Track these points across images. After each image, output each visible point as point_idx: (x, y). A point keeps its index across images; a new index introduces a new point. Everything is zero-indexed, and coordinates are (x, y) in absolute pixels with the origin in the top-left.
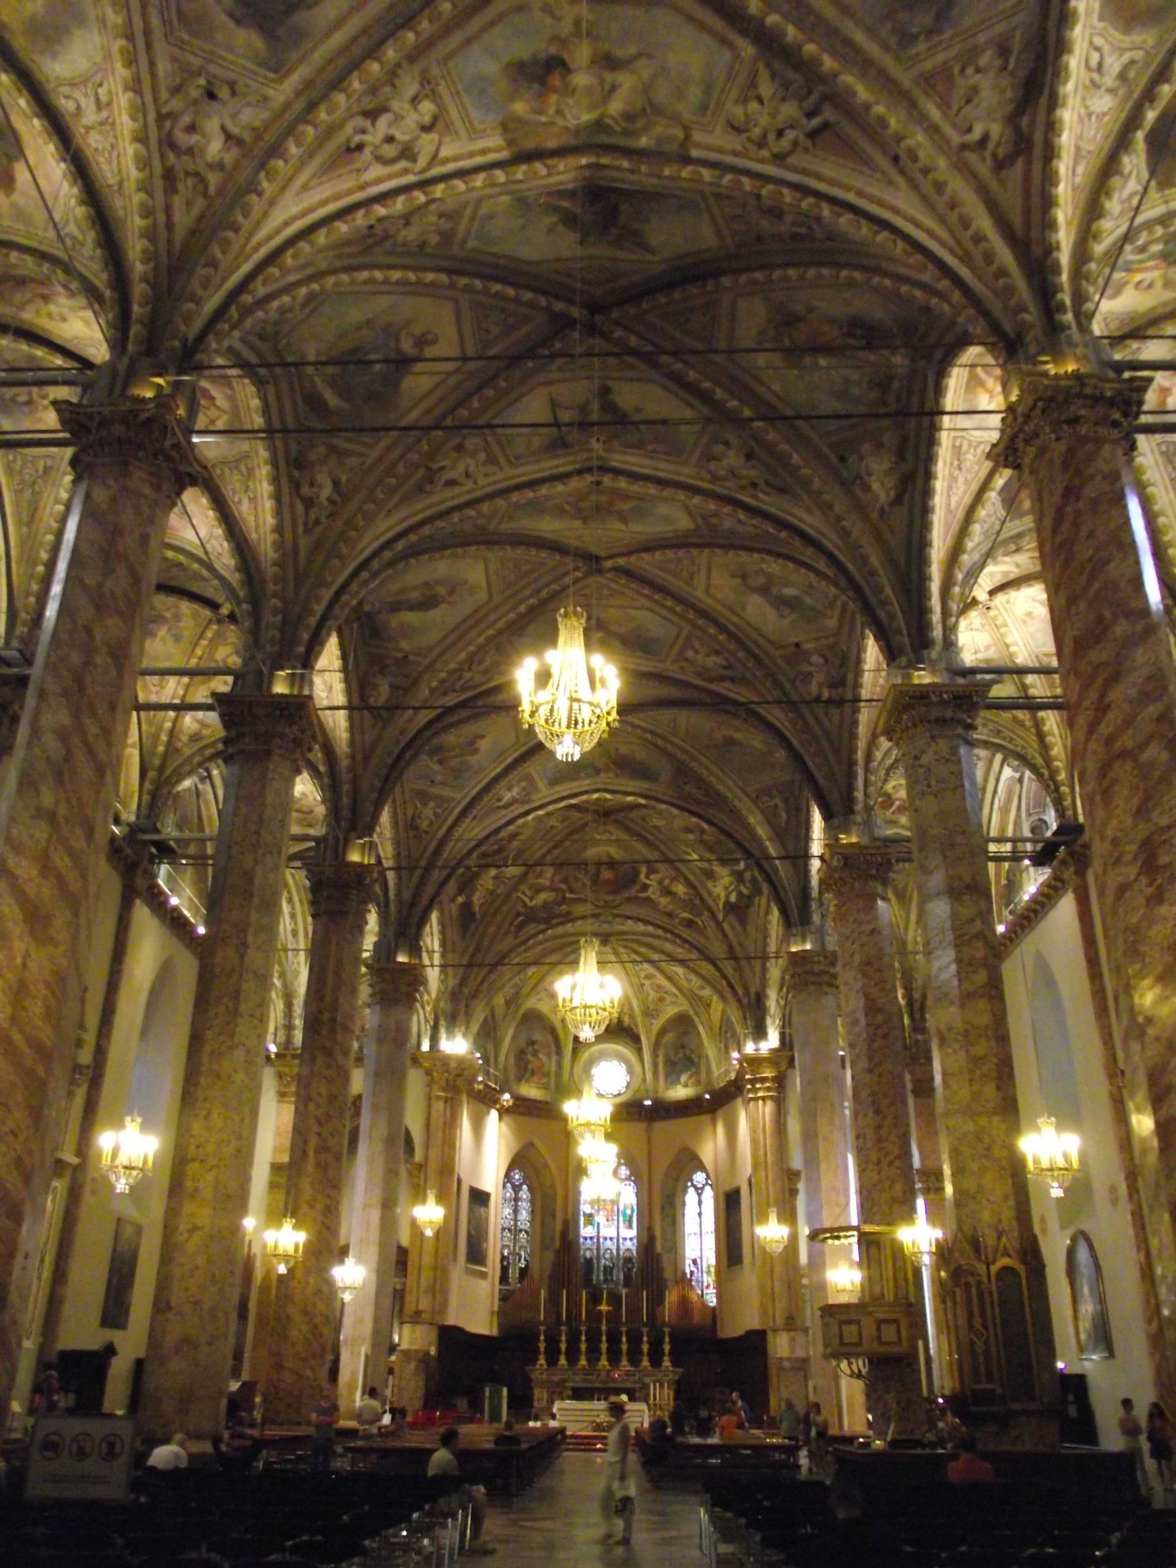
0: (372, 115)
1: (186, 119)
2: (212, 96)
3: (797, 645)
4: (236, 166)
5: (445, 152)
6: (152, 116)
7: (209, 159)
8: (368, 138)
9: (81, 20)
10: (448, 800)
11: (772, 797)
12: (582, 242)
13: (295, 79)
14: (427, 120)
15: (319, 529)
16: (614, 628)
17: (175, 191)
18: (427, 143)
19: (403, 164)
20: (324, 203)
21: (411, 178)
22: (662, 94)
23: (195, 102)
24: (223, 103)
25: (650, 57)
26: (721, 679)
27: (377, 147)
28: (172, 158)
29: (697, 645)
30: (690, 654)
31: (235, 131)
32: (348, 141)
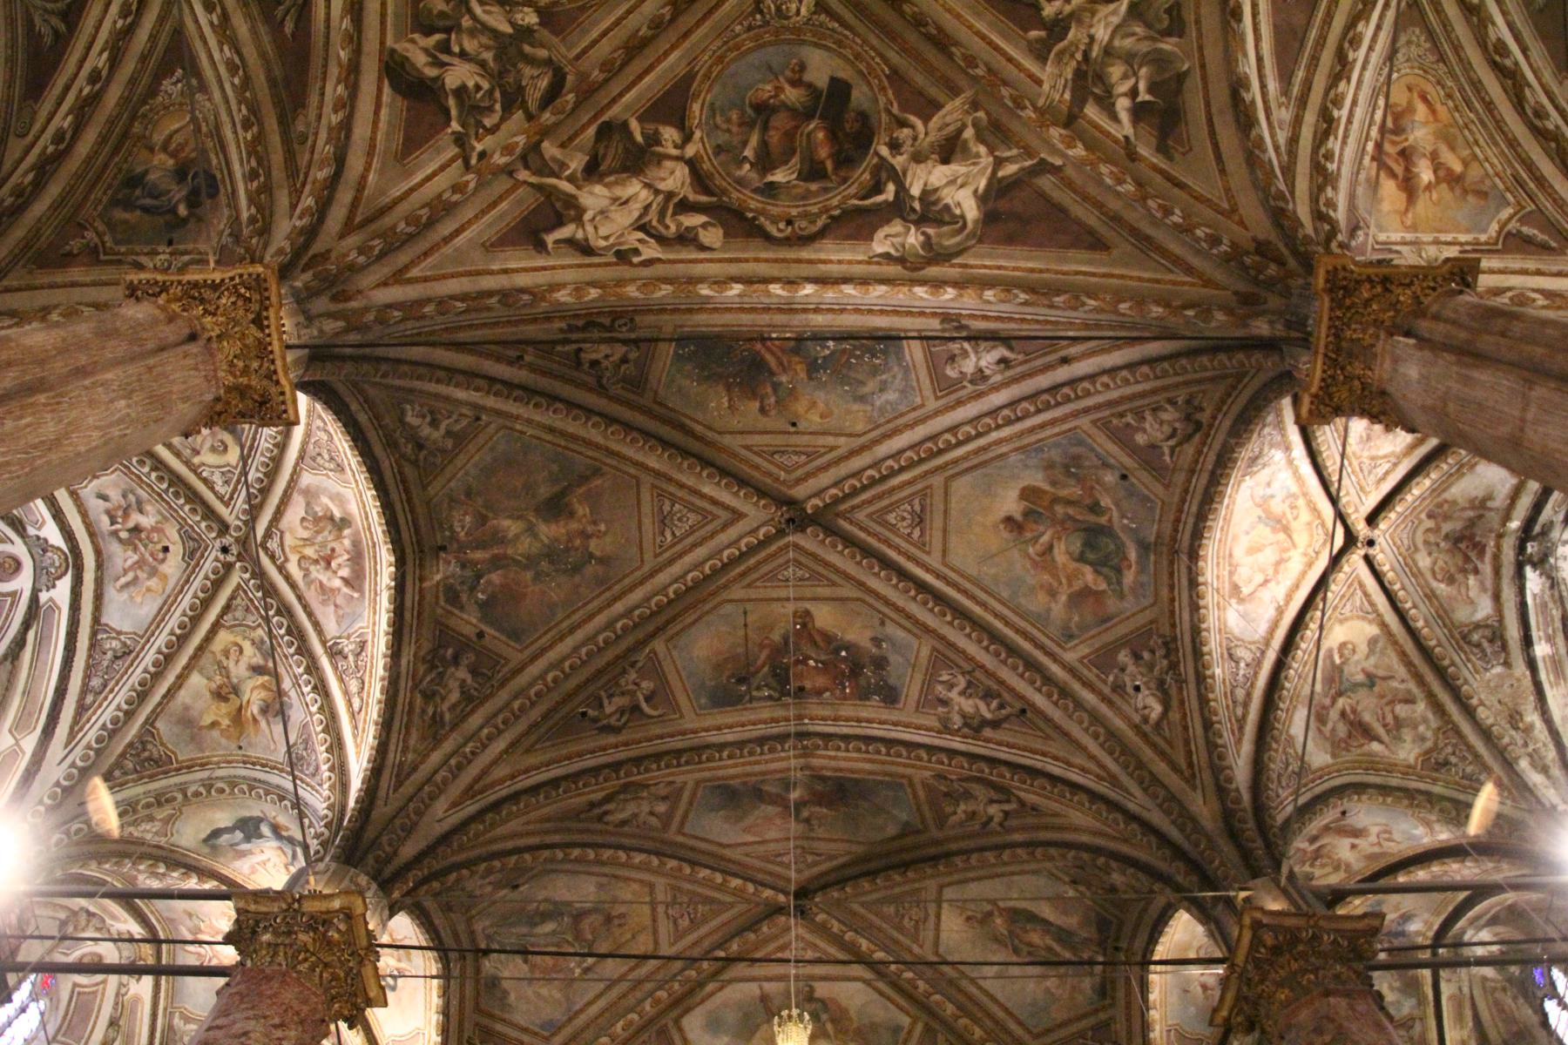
3: (516, 887)
10: (1103, 425)
11: (449, 433)
16: (771, 810)
26: (608, 799)
29: (654, 821)
30: (661, 808)
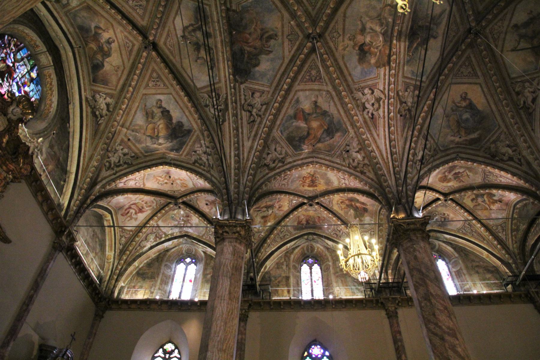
0: (365, 108)
1: (351, 161)
2: (348, 151)
4: (365, 153)
5: (382, 89)
6: (348, 169)
7: (361, 160)
8: (371, 111)
9: (326, 174)
12: (435, 38)
13: (349, 128)
14: (370, 92)
15: (522, 160)
17: (365, 173)
18: (377, 93)
19: (381, 102)
20: (384, 131)
21: (386, 101)
22: (374, 14)
23: (348, 156)
24: (351, 149)
25: (361, 17)
27: (374, 109)
28: (358, 169)
31: (357, 149)
32: (369, 117)
